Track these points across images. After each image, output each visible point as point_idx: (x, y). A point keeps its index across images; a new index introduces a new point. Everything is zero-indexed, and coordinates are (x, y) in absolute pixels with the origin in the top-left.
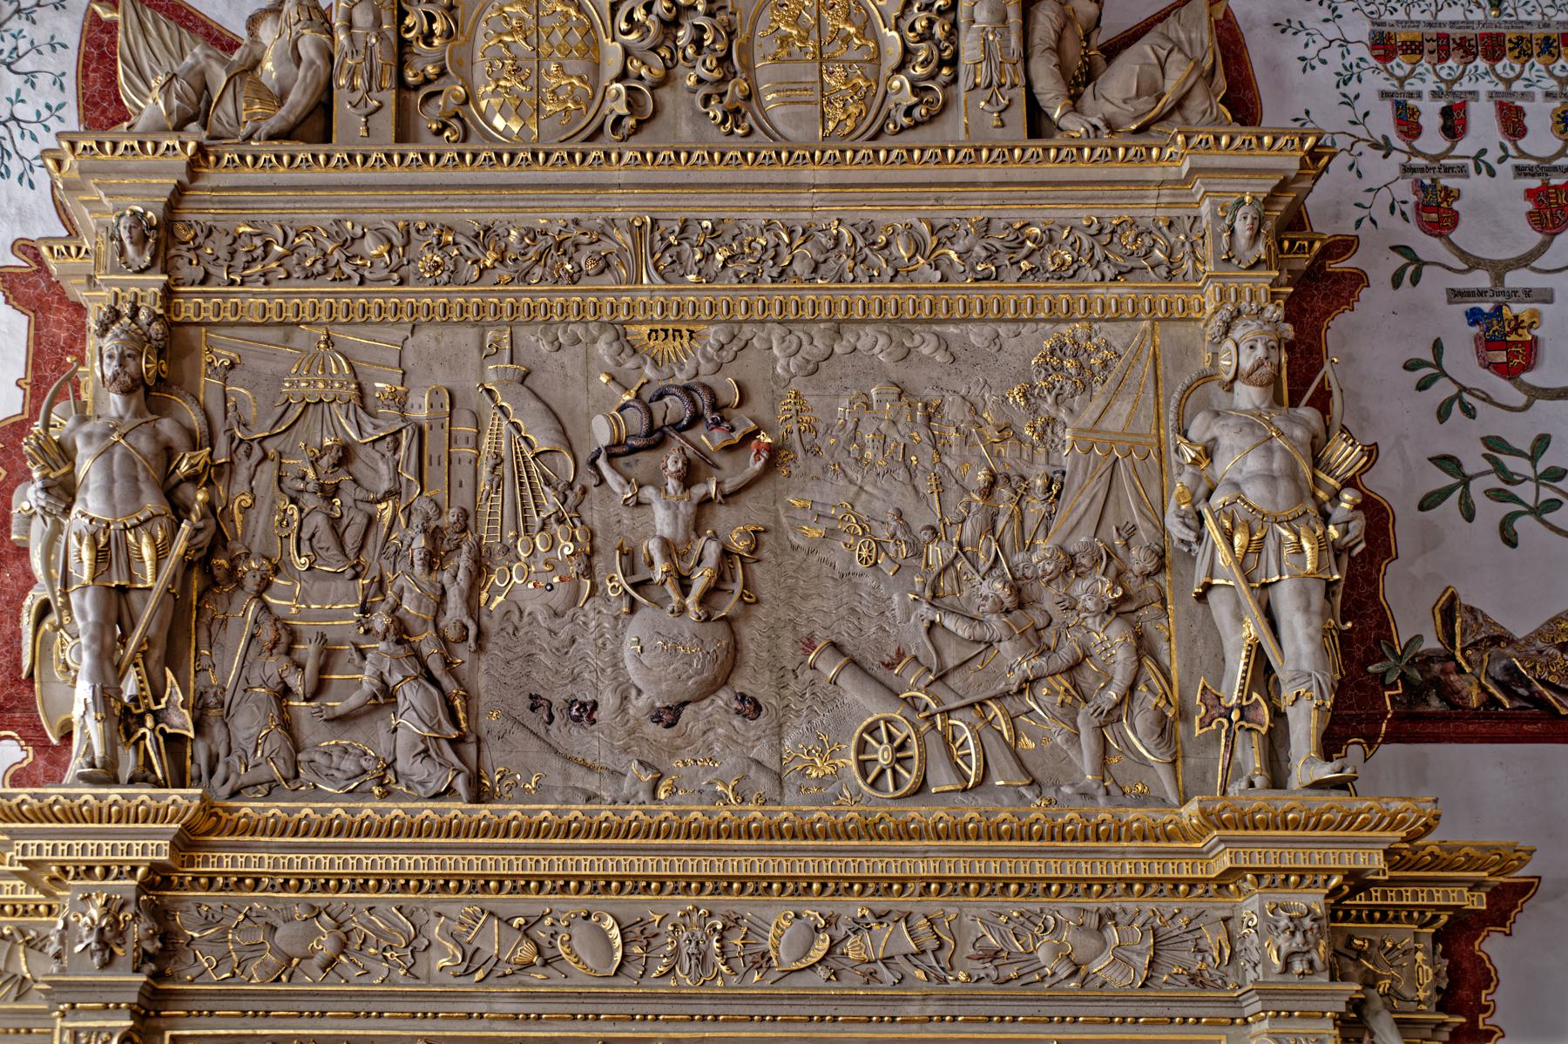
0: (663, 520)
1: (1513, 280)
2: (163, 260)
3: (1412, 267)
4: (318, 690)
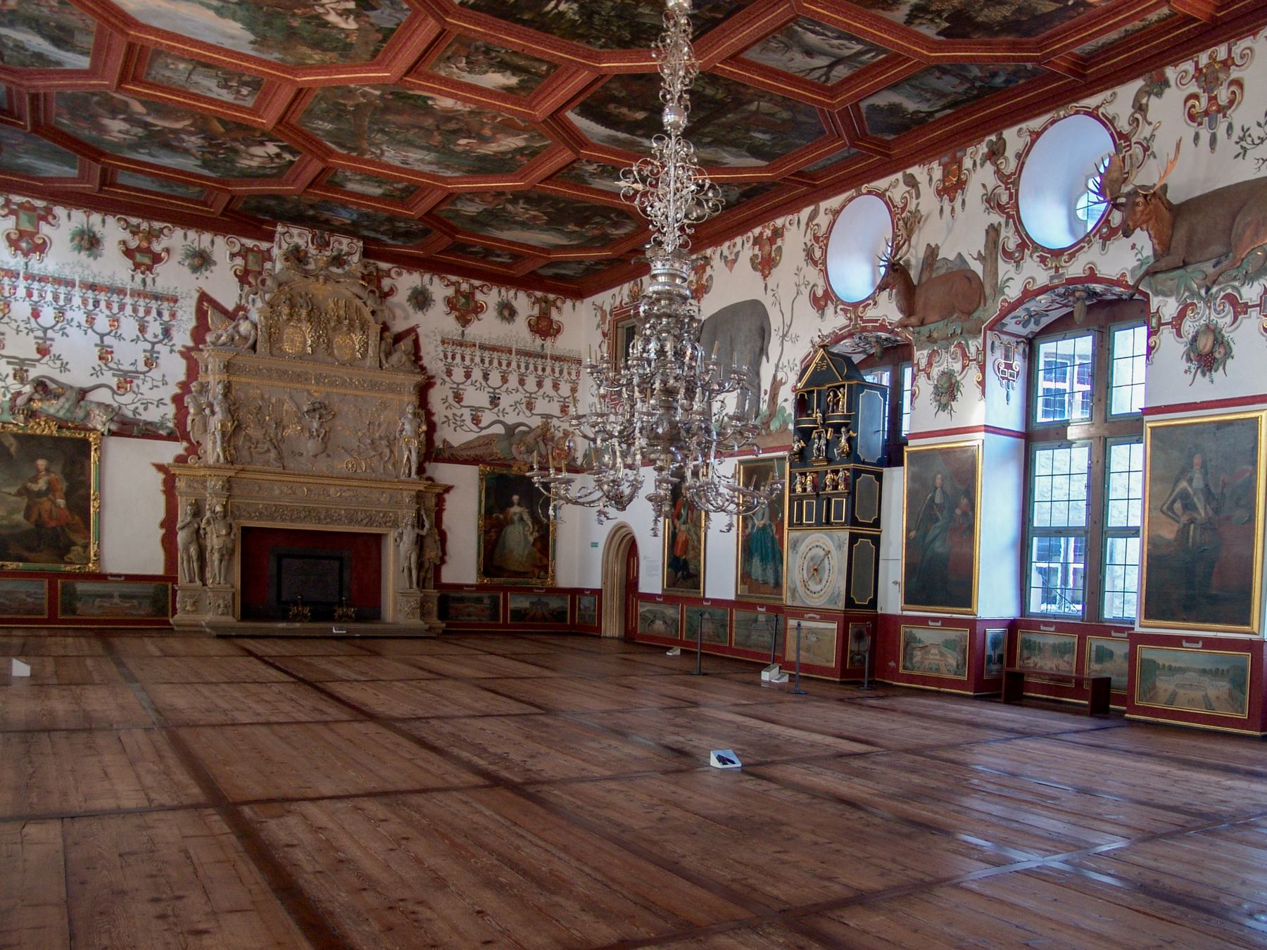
0: (315, 425)
1: (461, 386)
2: (227, 372)
3: (444, 382)
4: (256, 447)
